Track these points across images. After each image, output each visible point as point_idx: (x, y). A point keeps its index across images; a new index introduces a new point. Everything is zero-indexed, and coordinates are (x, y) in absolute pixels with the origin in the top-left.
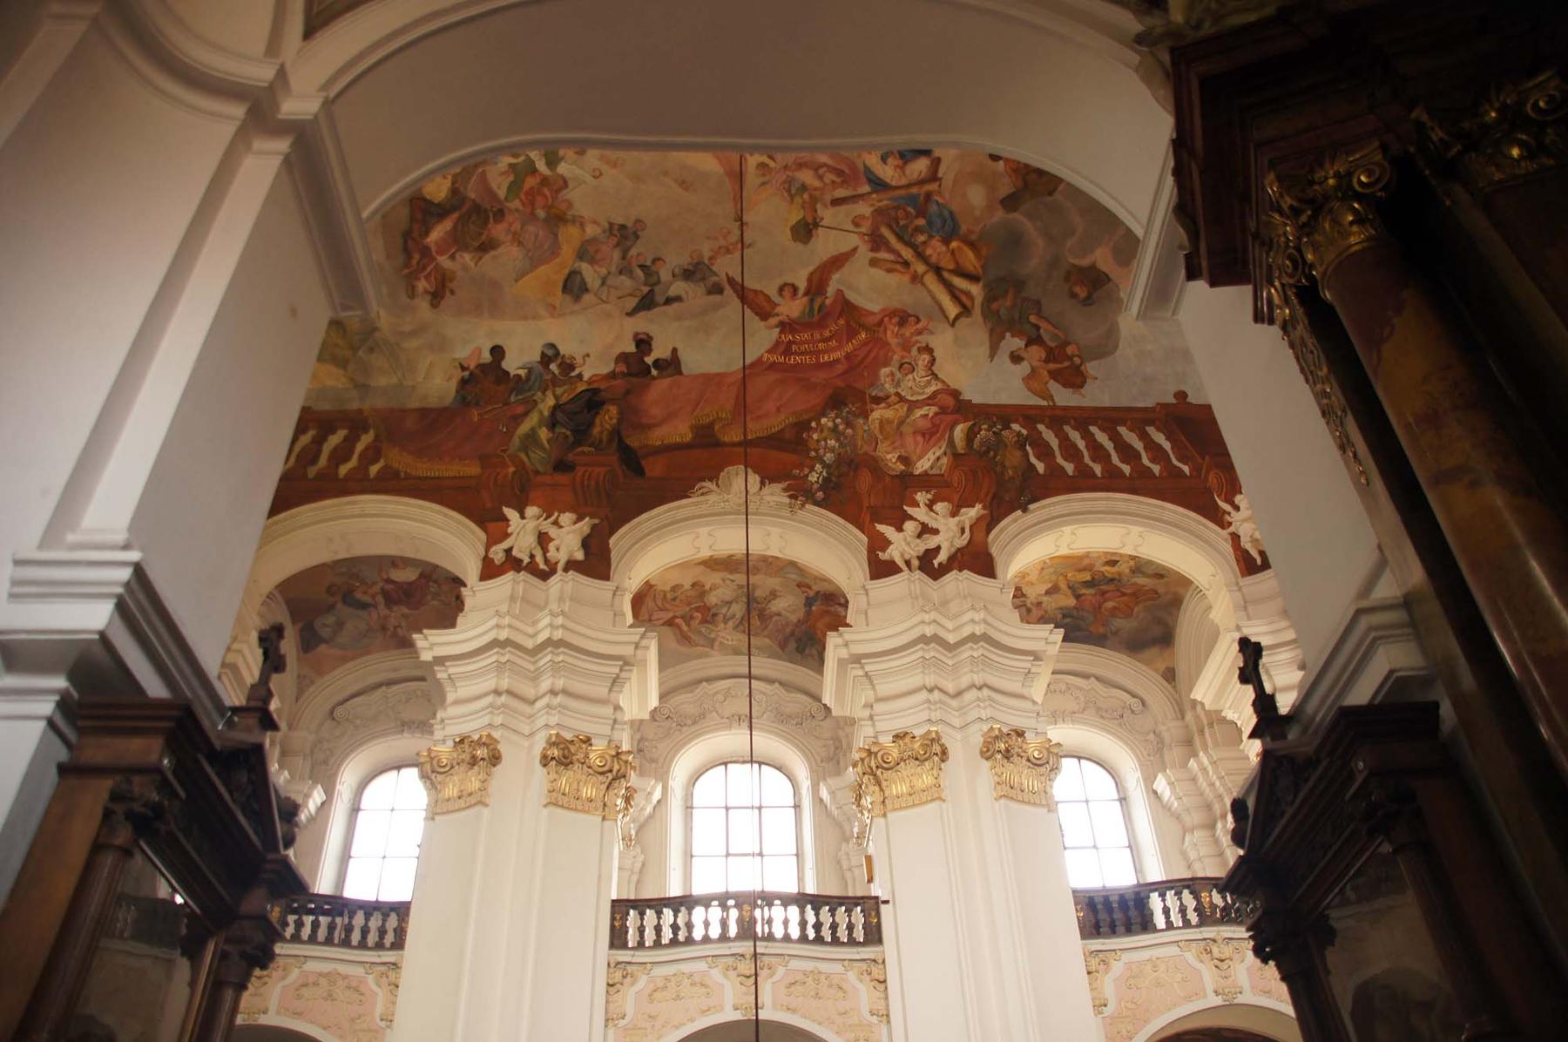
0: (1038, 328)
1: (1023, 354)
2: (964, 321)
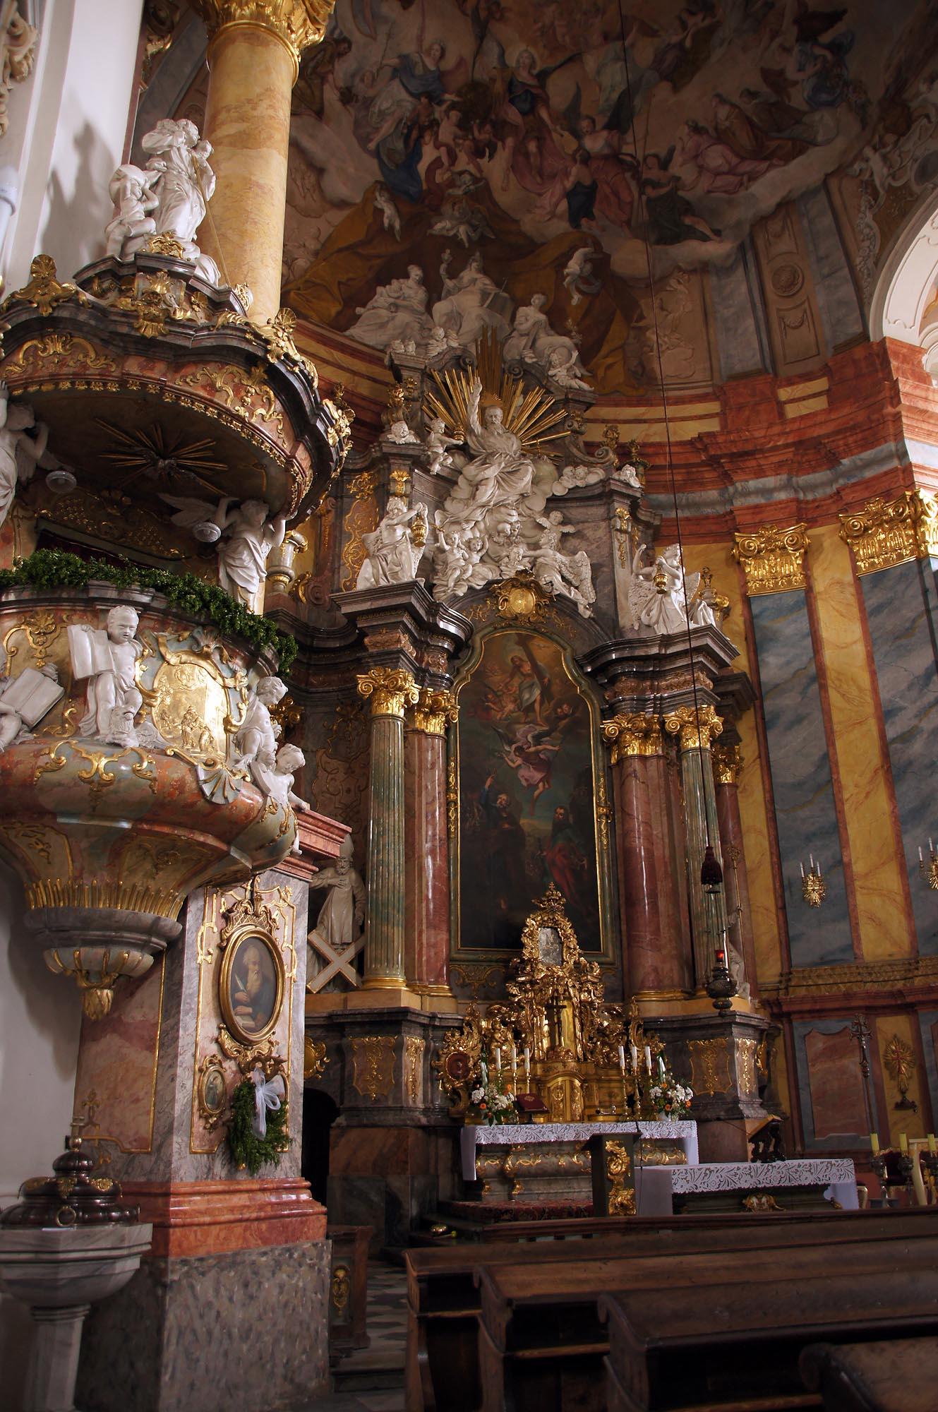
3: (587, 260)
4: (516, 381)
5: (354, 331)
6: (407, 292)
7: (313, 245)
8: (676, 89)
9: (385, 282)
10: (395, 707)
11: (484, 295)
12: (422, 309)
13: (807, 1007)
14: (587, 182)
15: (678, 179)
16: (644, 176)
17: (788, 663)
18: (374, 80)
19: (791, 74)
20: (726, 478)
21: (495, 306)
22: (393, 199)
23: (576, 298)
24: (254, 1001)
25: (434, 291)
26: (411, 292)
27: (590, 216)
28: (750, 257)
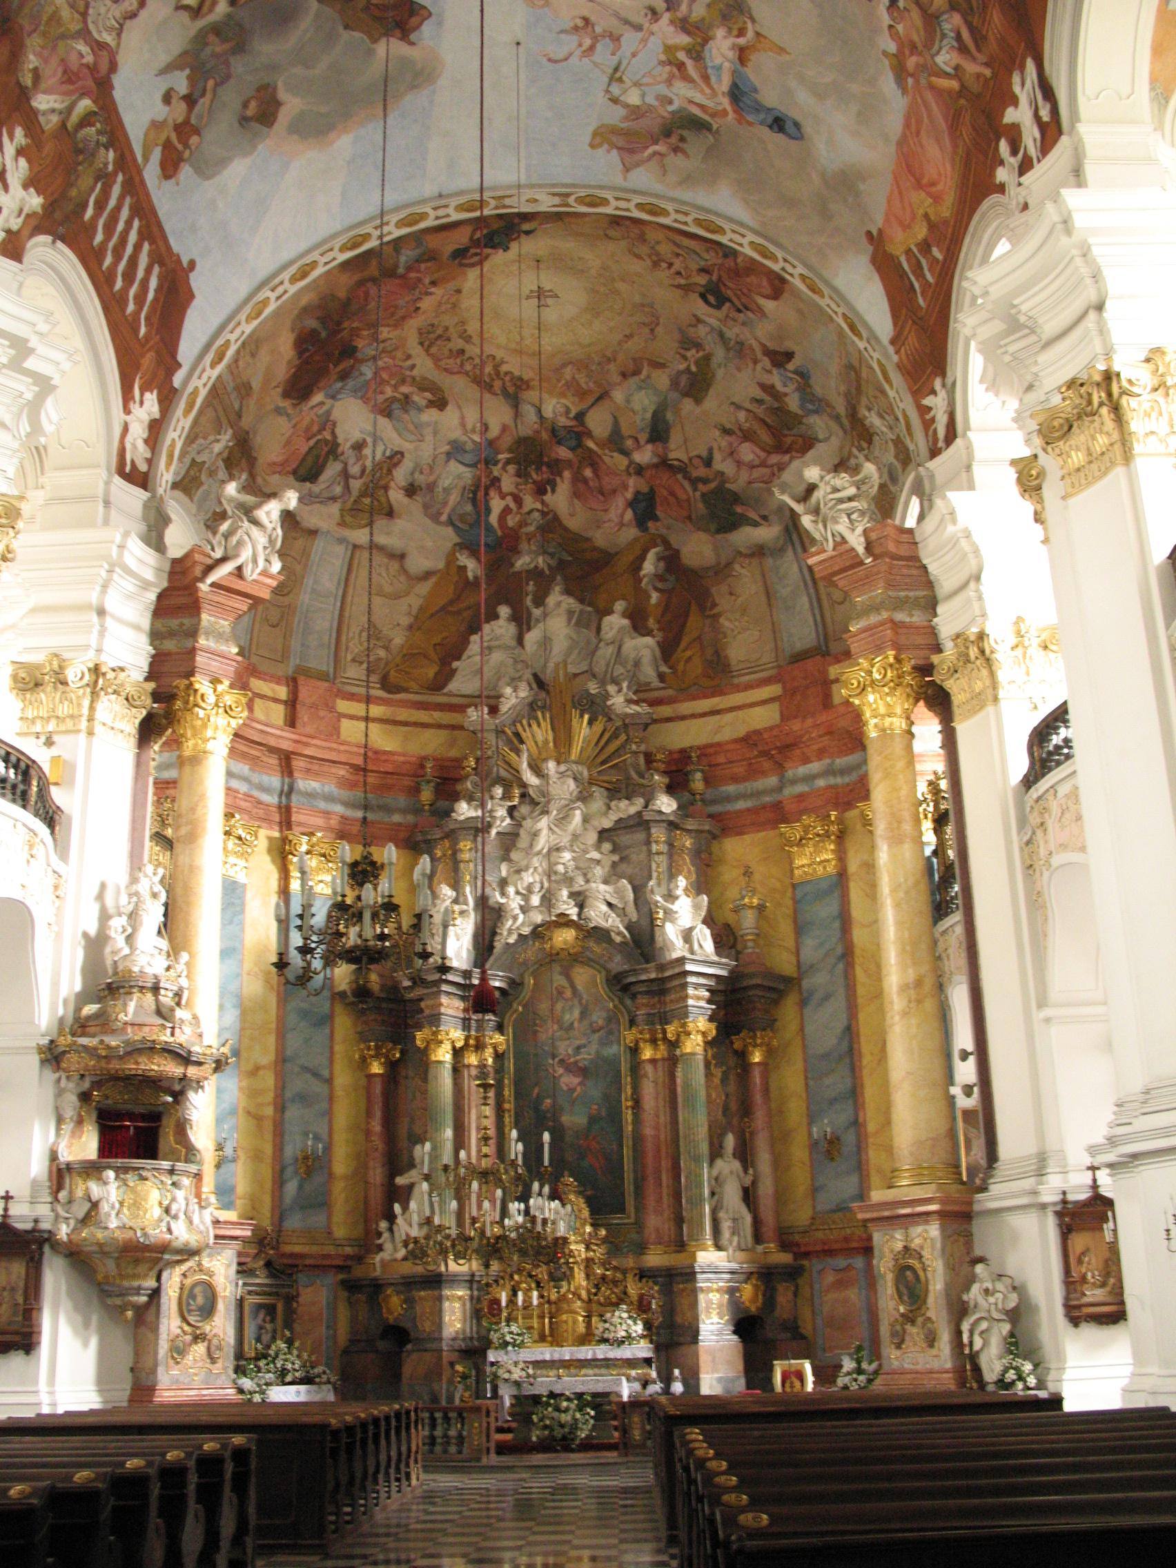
0: (203, 94)
1: (174, 101)
2: (184, 16)
3: (660, 558)
4: (582, 716)
5: (453, 686)
6: (499, 631)
7: (405, 621)
8: (698, 401)
9: (475, 628)
10: (444, 1054)
11: (570, 613)
12: (514, 643)
13: (818, 1248)
14: (645, 489)
15: (722, 474)
16: (695, 474)
17: (821, 944)
18: (431, 468)
19: (779, 387)
20: (780, 767)
21: (580, 622)
22: (474, 553)
23: (655, 597)
24: (201, 1309)
25: (522, 621)
26: (502, 631)
27: (655, 518)
28: (795, 537)
